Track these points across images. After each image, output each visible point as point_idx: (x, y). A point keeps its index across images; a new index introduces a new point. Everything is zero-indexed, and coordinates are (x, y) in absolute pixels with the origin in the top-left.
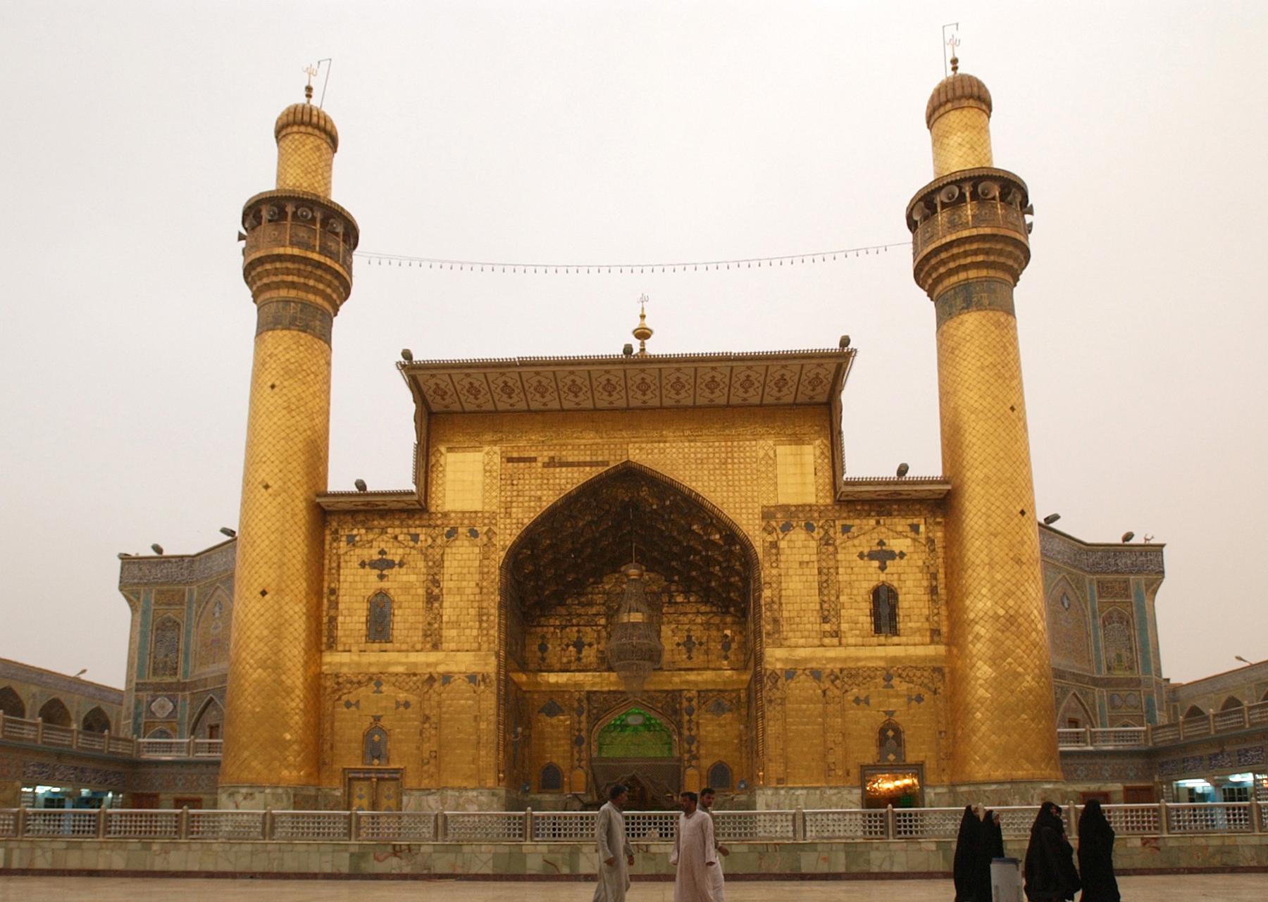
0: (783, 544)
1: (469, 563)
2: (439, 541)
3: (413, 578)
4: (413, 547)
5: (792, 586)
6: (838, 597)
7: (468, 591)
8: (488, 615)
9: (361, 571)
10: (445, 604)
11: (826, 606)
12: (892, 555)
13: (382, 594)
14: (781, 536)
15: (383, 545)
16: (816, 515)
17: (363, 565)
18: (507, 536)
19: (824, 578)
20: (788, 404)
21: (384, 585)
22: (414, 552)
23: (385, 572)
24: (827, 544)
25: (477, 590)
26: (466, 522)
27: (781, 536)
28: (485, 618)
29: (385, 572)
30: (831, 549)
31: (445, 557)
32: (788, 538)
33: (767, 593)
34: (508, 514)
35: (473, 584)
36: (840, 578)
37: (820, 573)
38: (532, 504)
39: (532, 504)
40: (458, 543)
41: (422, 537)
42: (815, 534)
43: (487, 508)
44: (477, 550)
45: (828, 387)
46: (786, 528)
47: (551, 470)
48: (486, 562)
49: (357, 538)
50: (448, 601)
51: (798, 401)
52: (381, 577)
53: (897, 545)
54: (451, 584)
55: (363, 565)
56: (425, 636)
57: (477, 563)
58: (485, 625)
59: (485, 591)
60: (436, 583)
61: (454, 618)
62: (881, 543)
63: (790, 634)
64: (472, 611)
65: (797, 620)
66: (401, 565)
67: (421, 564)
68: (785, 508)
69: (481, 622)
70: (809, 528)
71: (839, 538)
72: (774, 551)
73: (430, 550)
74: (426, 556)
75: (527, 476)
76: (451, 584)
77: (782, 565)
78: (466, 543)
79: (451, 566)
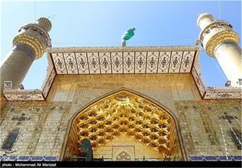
0: (186, 113)
1: (57, 119)
2: (47, 111)
3: (32, 124)
4: (36, 113)
5: (194, 129)
6: (215, 133)
7: (53, 130)
8: (59, 140)
9: (12, 121)
10: (42, 135)
11: (211, 137)
12: (232, 118)
13: (17, 130)
14: (185, 110)
15: (24, 112)
16: (196, 104)
17: (13, 119)
18: (74, 110)
19: (207, 126)
20: (177, 73)
21: (18, 127)
22: (36, 115)
23: (21, 122)
24: (204, 113)
25: (58, 129)
26: (59, 105)
27: (185, 110)
28: (57, 141)
29: (21, 122)
30: (206, 115)
31: (48, 117)
32: (187, 111)
33: (183, 132)
34: (76, 103)
35: (56, 127)
36: (214, 126)
37: (204, 124)
38: (86, 100)
39: (86, 100)
40: (54, 112)
41: (41, 110)
42: (198, 110)
43: (68, 101)
44: (61, 114)
45: (191, 65)
46: (186, 108)
47: (95, 90)
48: (63, 119)
49: (15, 110)
50: (44, 132)
51: (180, 72)
52: (19, 124)
53: (231, 114)
54: (47, 127)
55: (13, 119)
56: (28, 148)
57: (60, 119)
58: (56, 144)
59: (60, 129)
60: (41, 126)
61: (43, 141)
62: (225, 113)
63: (199, 150)
64: (52, 138)
65: (200, 143)
66: (28, 119)
67: (37, 119)
68: (184, 102)
69: (55, 142)
70: (194, 107)
71: (209, 112)
72: (183, 116)
73: (42, 114)
74: (40, 116)
75: (86, 91)
76: (47, 127)
77: (188, 121)
78: (58, 112)
79: (49, 120)
